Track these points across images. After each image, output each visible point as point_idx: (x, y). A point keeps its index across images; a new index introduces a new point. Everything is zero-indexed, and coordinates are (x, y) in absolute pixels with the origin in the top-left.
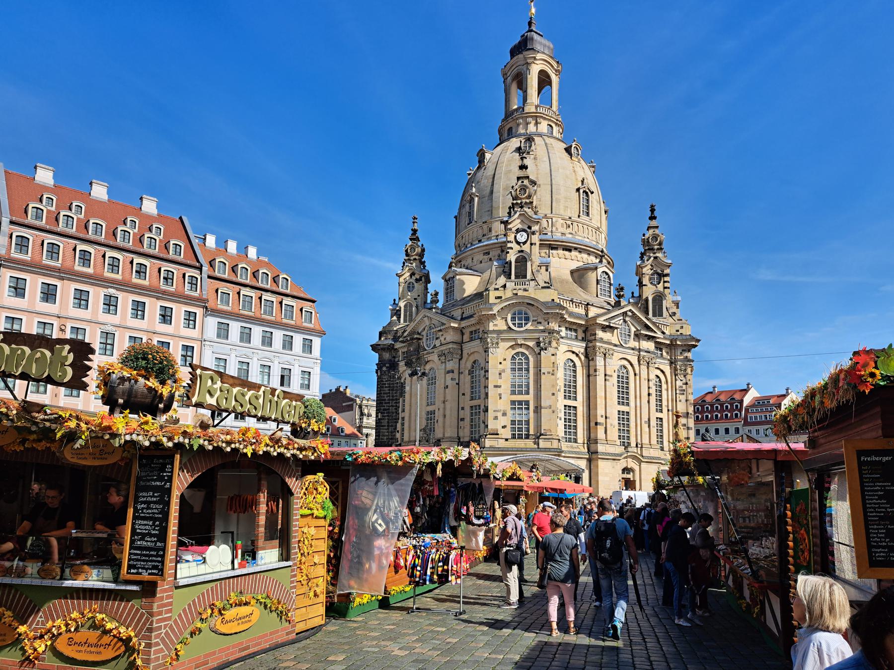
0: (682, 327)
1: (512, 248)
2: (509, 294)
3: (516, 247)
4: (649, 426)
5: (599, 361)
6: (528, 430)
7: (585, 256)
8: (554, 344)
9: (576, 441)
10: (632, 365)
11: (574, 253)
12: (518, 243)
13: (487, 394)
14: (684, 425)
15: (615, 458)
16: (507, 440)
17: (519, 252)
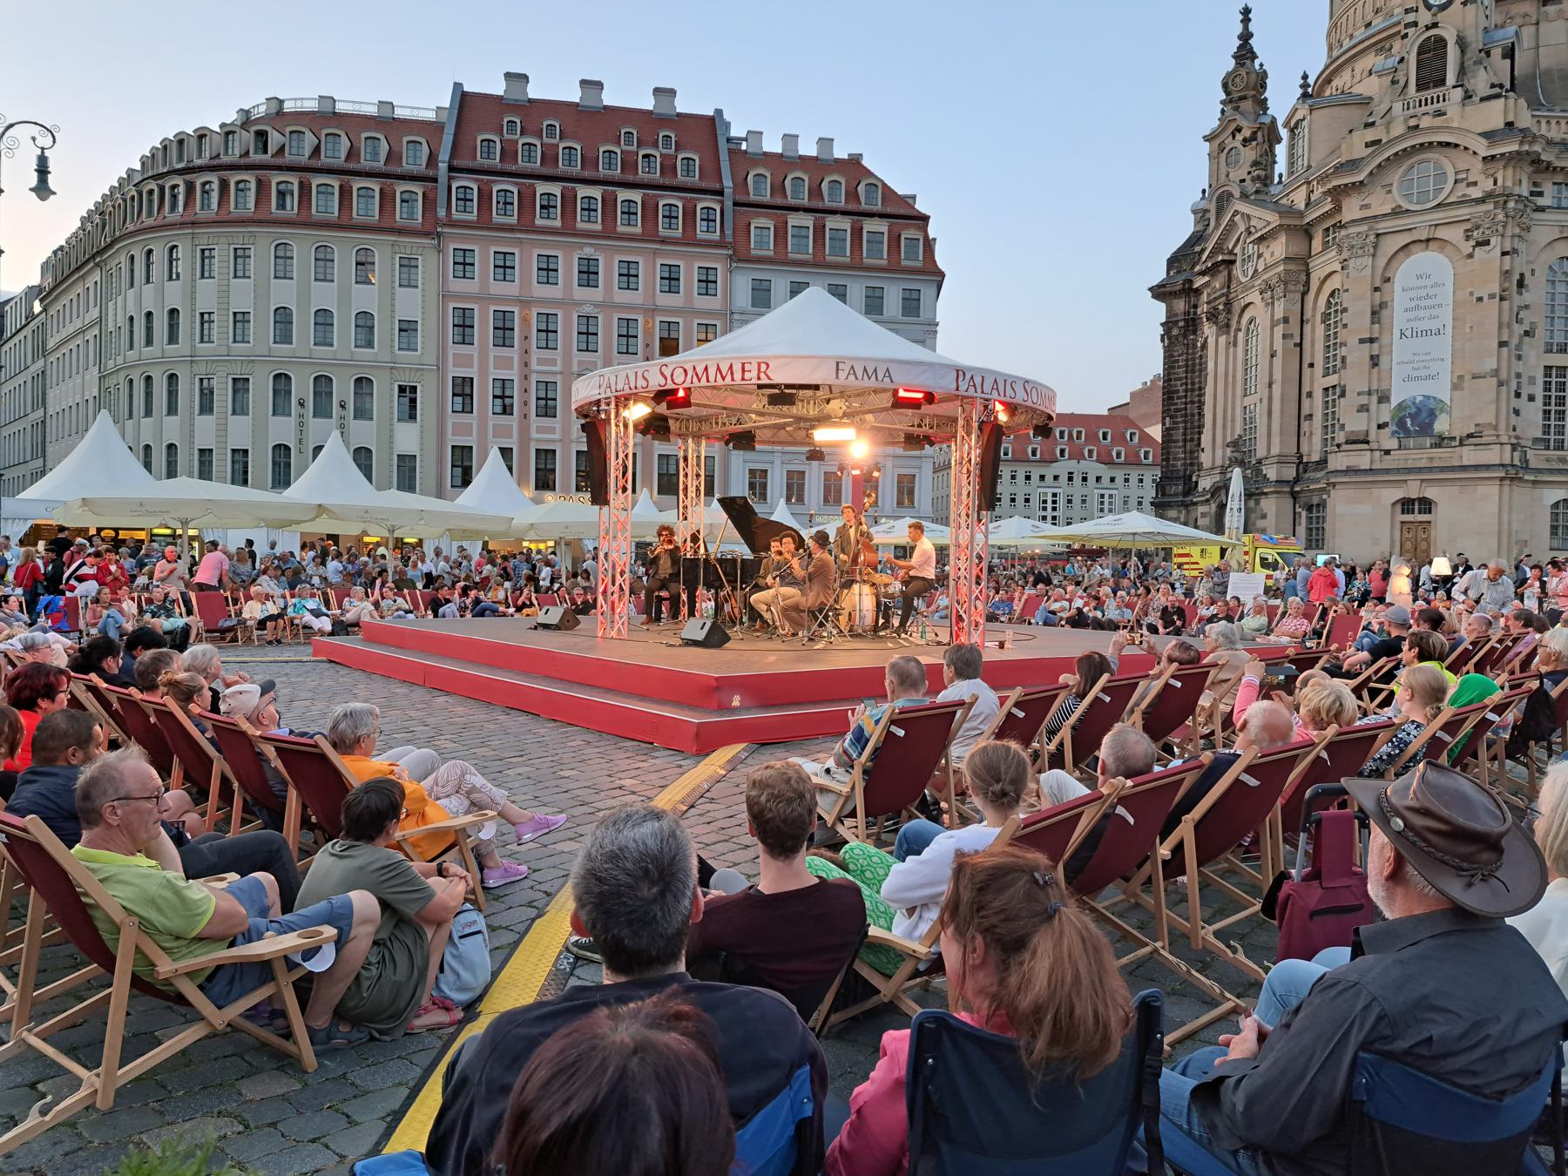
1: (1415, 24)
2: (1398, 129)
3: (1425, 17)
12: (1429, 7)
13: (1344, 359)
16: (1387, 452)
17: (1428, 28)
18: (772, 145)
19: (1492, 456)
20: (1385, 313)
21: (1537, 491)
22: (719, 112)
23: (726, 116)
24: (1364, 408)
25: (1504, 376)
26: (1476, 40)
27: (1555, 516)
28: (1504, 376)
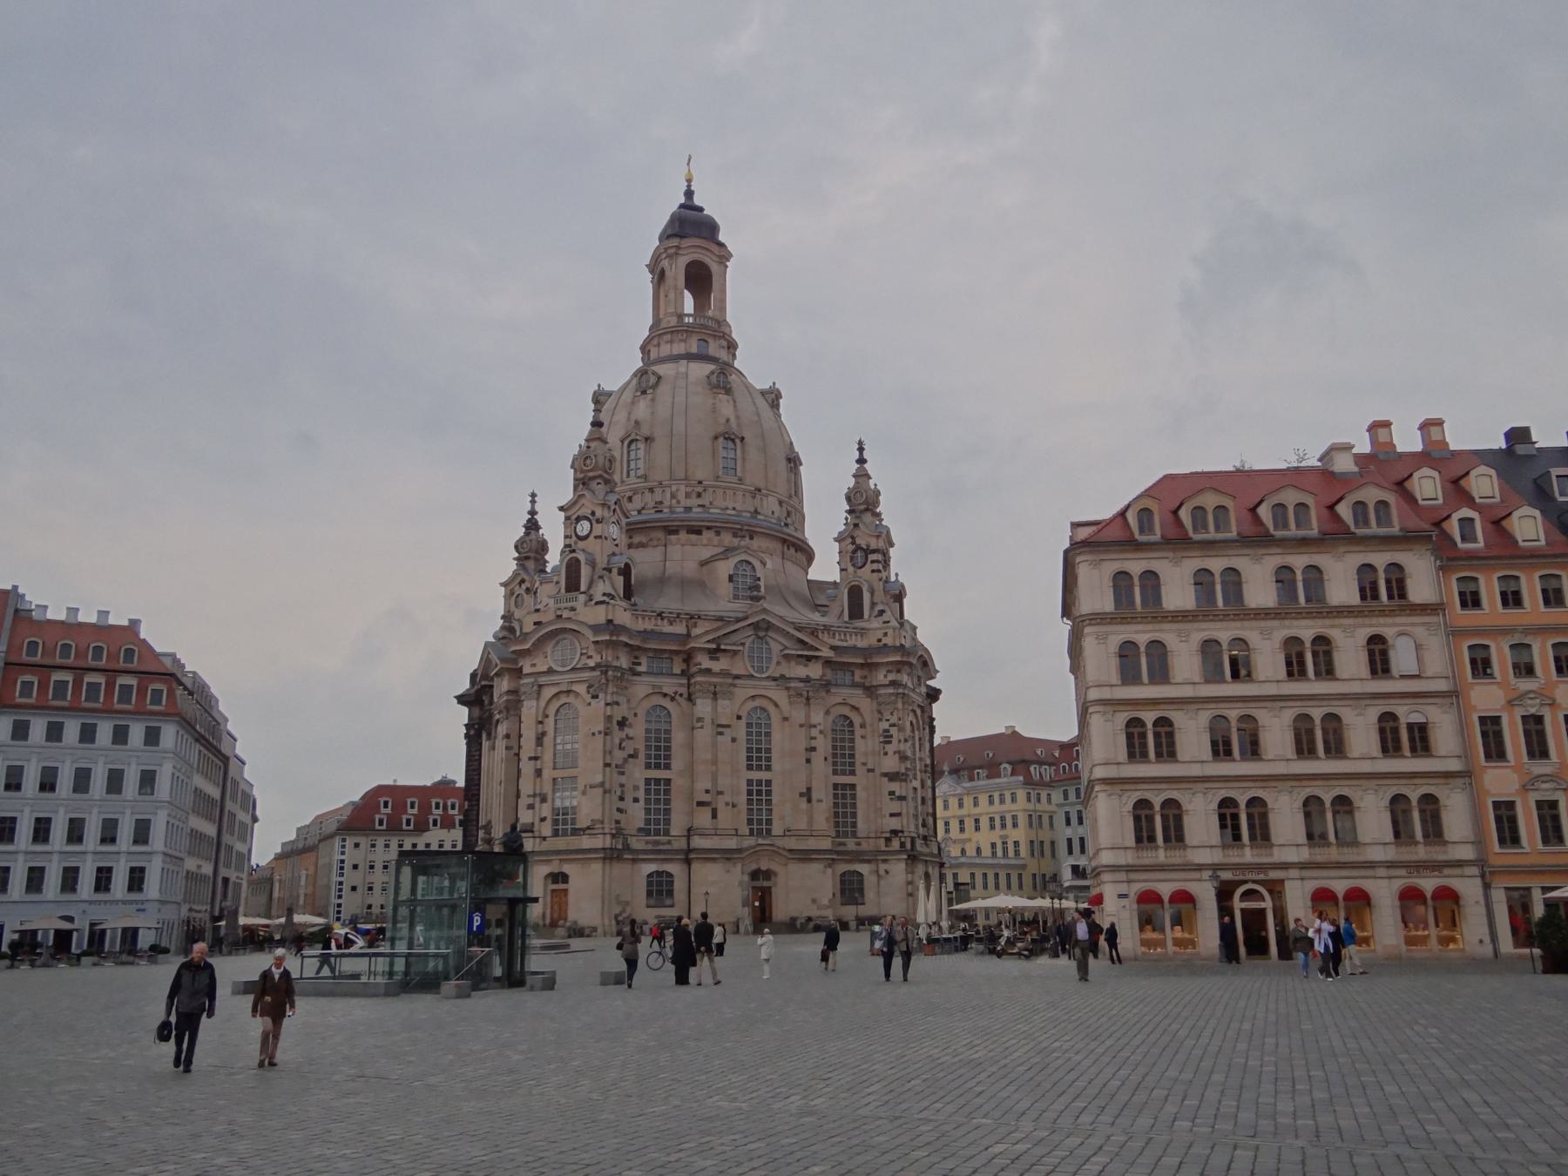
0: (886, 634)
2: (551, 617)
4: (809, 801)
5: (703, 707)
6: (574, 821)
7: (727, 539)
8: (611, 689)
9: (667, 833)
10: (776, 705)
11: (707, 535)
14: (892, 793)
15: (728, 856)
16: (545, 839)
18: (56, 613)
19: (598, 842)
20: (546, 739)
21: (637, 866)
22: (15, 588)
23: (21, 591)
24: (531, 807)
25: (607, 786)
26: (602, 562)
27: (649, 884)
28: (607, 786)
